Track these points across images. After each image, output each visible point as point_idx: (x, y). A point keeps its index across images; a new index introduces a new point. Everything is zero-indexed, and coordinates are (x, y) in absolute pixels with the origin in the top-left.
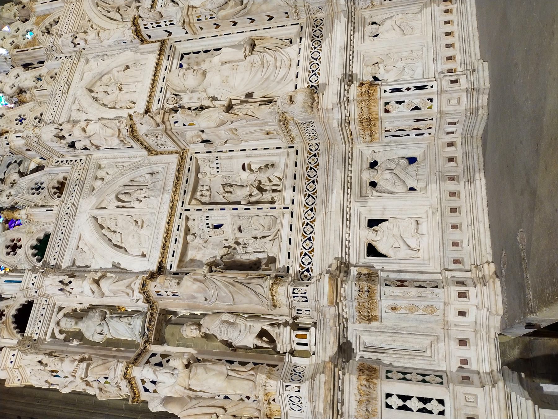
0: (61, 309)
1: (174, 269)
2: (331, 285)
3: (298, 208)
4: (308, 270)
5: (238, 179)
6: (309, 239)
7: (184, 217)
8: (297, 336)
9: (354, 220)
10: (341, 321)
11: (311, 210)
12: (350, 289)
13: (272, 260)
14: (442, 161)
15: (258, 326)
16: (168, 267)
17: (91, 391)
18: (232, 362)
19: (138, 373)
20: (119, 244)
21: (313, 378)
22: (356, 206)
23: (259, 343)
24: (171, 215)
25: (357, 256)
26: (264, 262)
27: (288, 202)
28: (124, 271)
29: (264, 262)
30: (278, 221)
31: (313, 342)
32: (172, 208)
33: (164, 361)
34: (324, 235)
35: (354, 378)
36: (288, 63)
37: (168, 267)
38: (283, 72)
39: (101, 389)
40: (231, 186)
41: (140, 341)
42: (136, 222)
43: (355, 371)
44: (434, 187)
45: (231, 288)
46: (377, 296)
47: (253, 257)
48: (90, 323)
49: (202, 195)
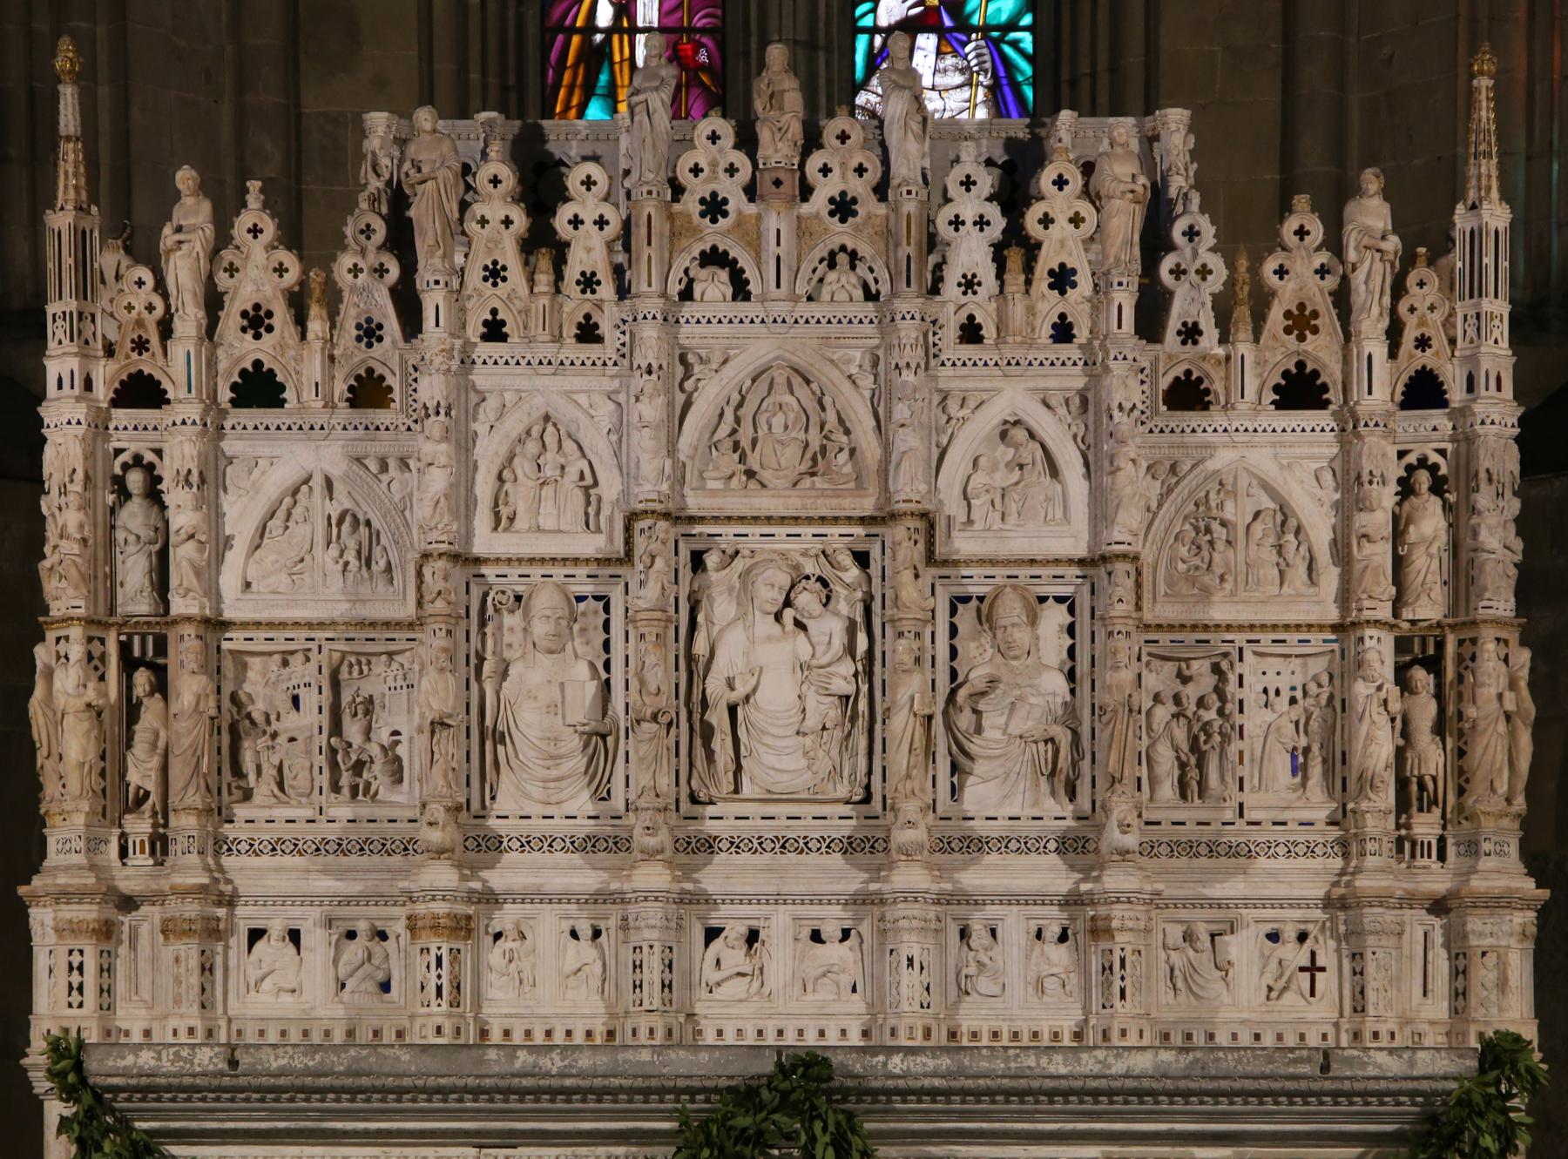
0: (159, 453)
1: (225, 645)
2: (193, 886)
3: (324, 830)
4: (229, 849)
5: (381, 723)
6: (274, 849)
7: (310, 645)
8: (142, 842)
9: (296, 911)
10: (157, 898)
11: (318, 849)
12: (191, 909)
13: (247, 795)
14: (376, 1023)
15: (151, 785)
16: (228, 635)
17: (47, 550)
18: (103, 758)
19: (76, 632)
20: (267, 534)
21: (92, 867)
22: (315, 913)
23: (131, 789)
24: (310, 625)
25: (246, 917)
26: (242, 783)
27: (333, 812)
28: (219, 559)
29: (242, 783)
30: (304, 800)
31: (136, 863)
32: (321, 625)
33: (96, 662)
34: (277, 870)
35: (94, 915)
36: (553, 799)
37: (228, 635)
38: (536, 791)
39: (51, 568)
40: (368, 712)
41: (118, 619)
42: (302, 560)
43: (103, 916)
44: (340, 1012)
45: (191, 751)
46: (185, 940)
47: (248, 765)
48: (140, 519)
49: (351, 666)
